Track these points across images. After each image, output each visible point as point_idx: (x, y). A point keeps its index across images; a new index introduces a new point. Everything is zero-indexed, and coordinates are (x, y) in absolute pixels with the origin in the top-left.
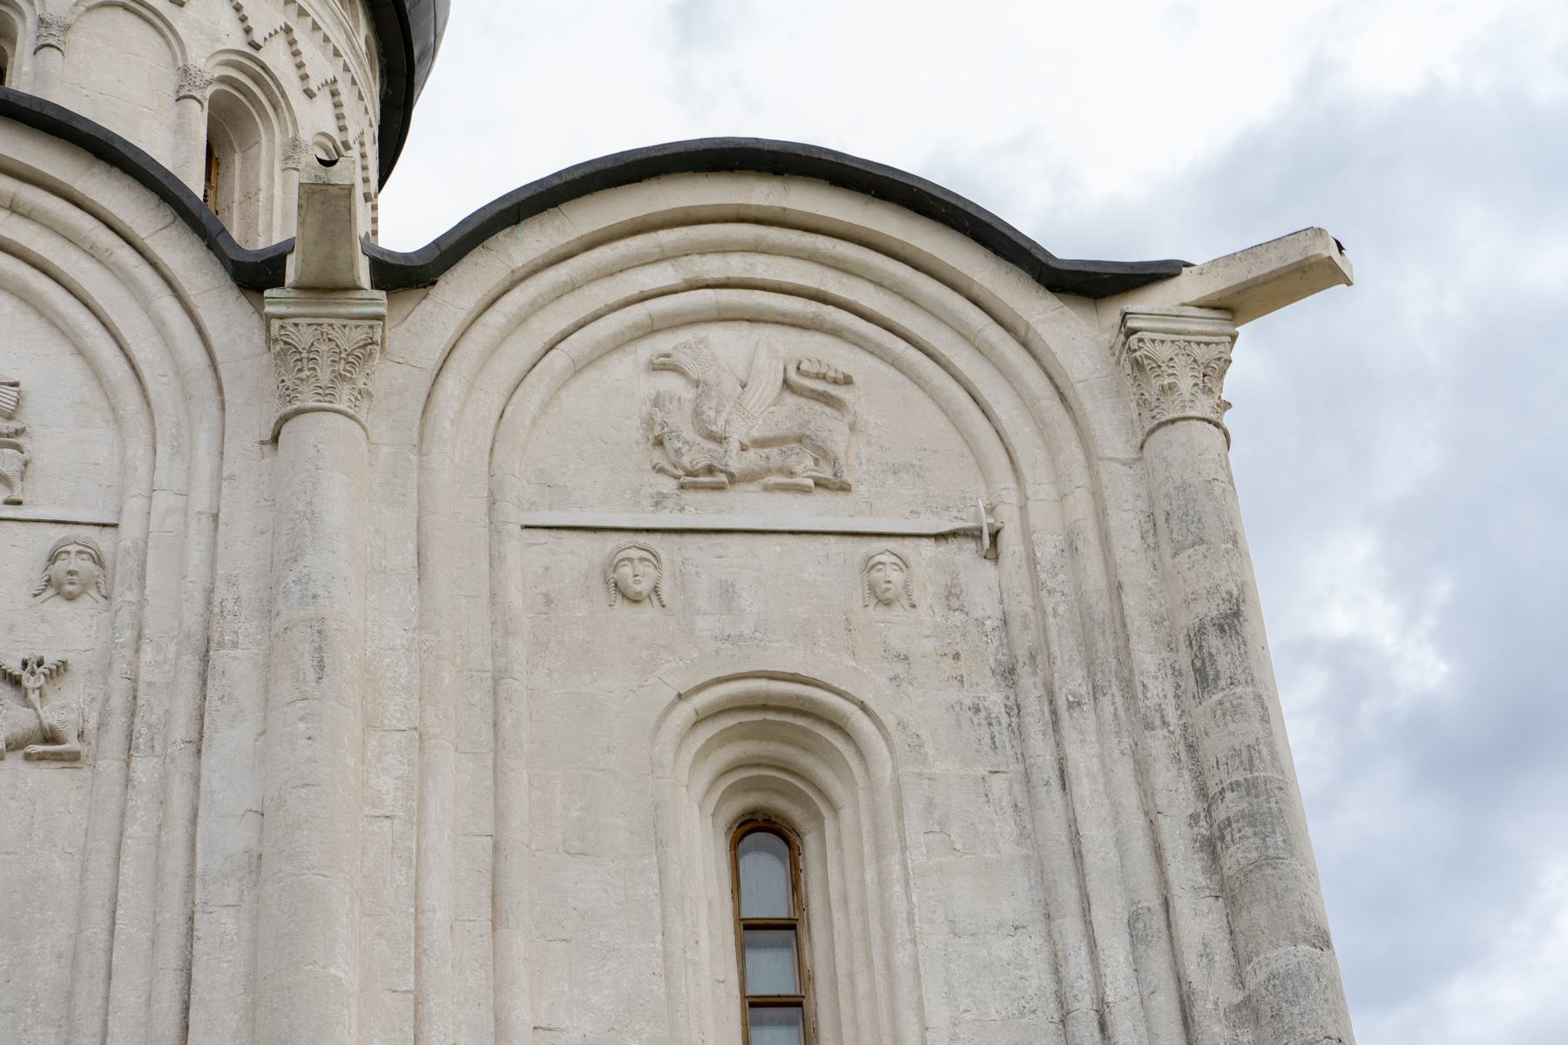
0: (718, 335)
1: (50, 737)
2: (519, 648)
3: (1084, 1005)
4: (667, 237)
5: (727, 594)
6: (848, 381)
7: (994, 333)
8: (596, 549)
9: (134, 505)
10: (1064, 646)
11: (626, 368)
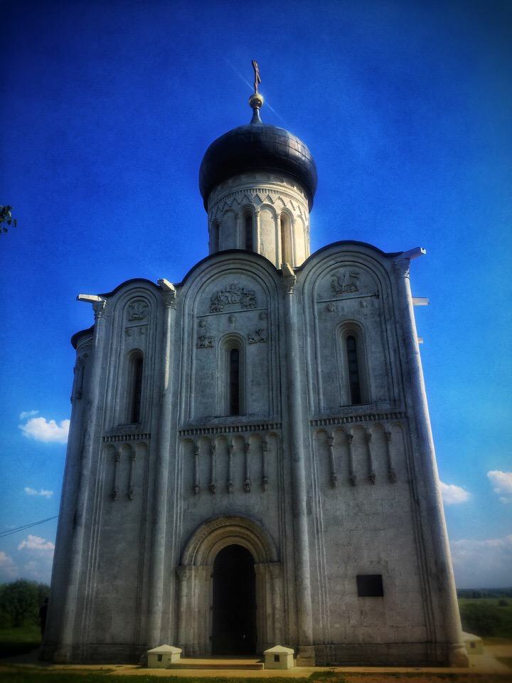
0: (340, 269)
1: (263, 339)
2: (317, 321)
3: (388, 362)
4: (333, 256)
5: (343, 308)
6: (358, 274)
7: (378, 265)
8: (324, 305)
9: (269, 306)
10: (386, 311)
11: (328, 276)
